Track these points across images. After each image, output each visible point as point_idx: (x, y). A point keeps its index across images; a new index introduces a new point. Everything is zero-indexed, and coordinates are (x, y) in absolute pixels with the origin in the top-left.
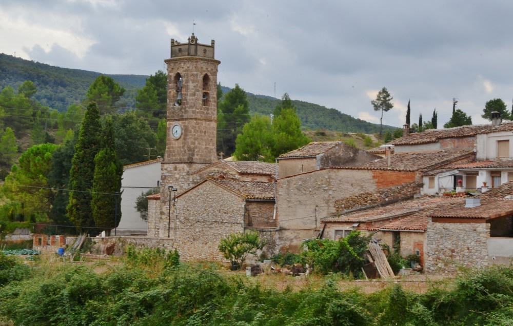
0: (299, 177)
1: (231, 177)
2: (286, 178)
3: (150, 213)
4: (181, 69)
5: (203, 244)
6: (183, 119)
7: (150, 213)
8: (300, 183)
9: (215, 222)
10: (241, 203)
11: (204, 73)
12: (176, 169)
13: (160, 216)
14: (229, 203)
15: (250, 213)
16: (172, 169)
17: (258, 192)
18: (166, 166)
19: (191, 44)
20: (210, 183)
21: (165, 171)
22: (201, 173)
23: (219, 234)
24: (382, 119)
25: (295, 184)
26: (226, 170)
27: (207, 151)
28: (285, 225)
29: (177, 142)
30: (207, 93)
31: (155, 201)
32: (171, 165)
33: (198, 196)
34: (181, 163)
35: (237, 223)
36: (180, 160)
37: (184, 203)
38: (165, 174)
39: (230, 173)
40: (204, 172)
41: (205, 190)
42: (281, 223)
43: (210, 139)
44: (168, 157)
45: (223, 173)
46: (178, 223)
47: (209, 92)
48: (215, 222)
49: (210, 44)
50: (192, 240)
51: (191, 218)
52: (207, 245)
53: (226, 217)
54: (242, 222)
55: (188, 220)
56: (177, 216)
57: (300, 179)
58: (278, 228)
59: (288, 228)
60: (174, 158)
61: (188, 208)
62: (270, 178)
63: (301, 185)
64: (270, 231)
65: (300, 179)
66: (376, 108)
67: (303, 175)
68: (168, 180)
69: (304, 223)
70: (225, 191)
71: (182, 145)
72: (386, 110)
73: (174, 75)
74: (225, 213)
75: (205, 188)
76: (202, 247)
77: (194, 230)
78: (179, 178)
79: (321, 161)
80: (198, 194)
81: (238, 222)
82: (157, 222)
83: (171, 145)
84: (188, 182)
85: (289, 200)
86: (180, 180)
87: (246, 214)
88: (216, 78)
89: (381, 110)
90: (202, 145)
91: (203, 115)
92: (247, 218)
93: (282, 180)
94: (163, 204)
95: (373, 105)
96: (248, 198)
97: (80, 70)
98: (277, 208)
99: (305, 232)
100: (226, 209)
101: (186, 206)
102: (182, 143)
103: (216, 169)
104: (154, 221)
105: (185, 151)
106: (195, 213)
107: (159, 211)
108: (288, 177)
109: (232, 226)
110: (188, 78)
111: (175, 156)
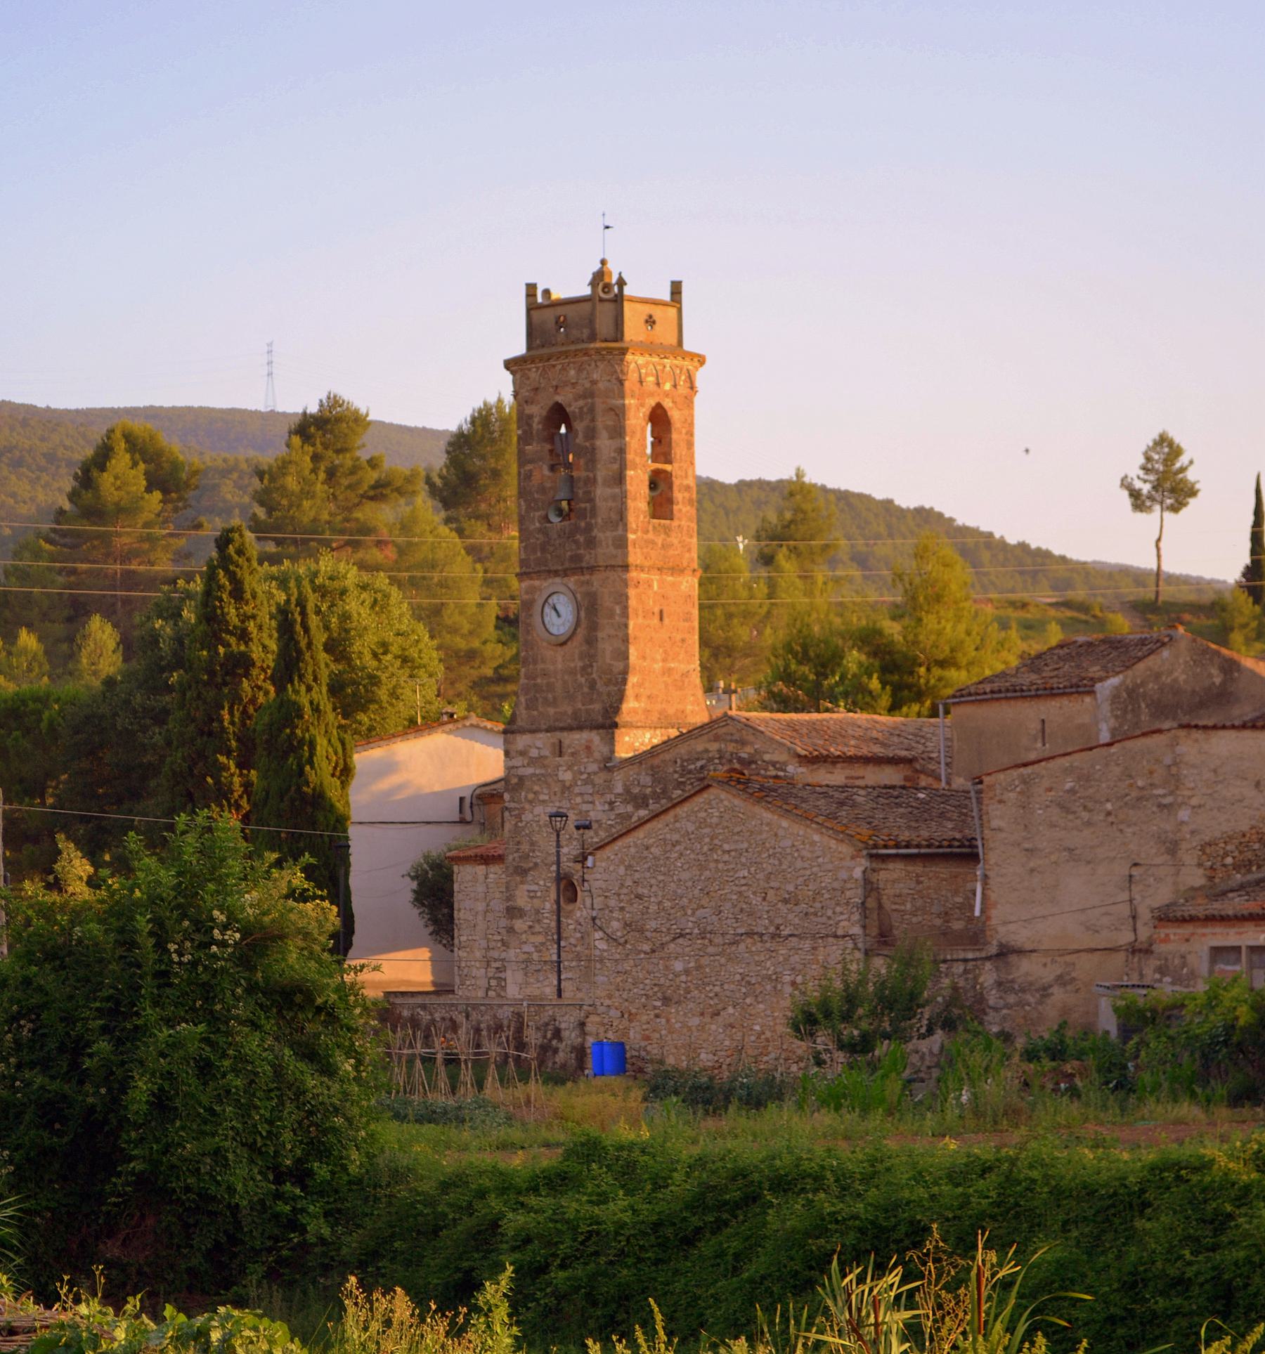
0: (1065, 762)
1: (773, 773)
2: (1017, 766)
3: (462, 915)
4: (568, 389)
5: (702, 1014)
6: (581, 570)
7: (462, 915)
8: (1068, 786)
9: (750, 934)
10: (848, 863)
11: (651, 402)
12: (560, 750)
13: (504, 922)
14: (799, 864)
15: (885, 900)
16: (546, 753)
17: (901, 821)
18: (522, 741)
19: (601, 300)
20: (723, 795)
21: (518, 761)
22: (656, 761)
23: (769, 977)
24: (1162, 545)
25: (1050, 790)
26: (749, 749)
27: (669, 681)
28: (1020, 936)
29: (560, 651)
30: (665, 471)
31: (481, 869)
32: (541, 735)
33: (678, 842)
34: (580, 728)
35: (836, 936)
36: (575, 715)
37: (622, 870)
38: (521, 771)
39: (767, 757)
40: (667, 757)
41: (702, 824)
42: (1002, 929)
43: (678, 637)
44: (527, 708)
45: (740, 760)
46: (602, 945)
47: (668, 467)
48: (750, 934)
49: (666, 296)
50: (658, 1004)
51: (652, 924)
52: (720, 1019)
53: (790, 916)
54: (856, 930)
55: (641, 931)
56: (594, 919)
57: (1068, 771)
58: (993, 950)
59: (1028, 947)
60: (551, 711)
61: (640, 890)
62: (909, 773)
63: (1072, 791)
64: (965, 960)
65: (1068, 771)
66: (1139, 501)
67: (1077, 756)
68: (531, 790)
69: (1088, 928)
70: (785, 823)
71: (580, 664)
72: (1175, 509)
73: (544, 413)
74: (786, 901)
75: (703, 814)
76: (701, 1028)
77: (667, 968)
78: (574, 783)
79: (1113, 703)
80: (676, 837)
81: (840, 932)
82: (492, 944)
83: (540, 666)
84: (609, 797)
85: (1027, 846)
86: (577, 790)
87: (871, 903)
88: (692, 416)
89: (1157, 508)
90: (654, 660)
91: (653, 553)
92: (875, 916)
93: (1001, 776)
94: (518, 879)
95: (1126, 493)
96: (875, 846)
97: (190, 409)
98: (986, 877)
99: (1096, 957)
100: (791, 888)
101: (629, 883)
102: (581, 658)
103: (714, 747)
104: (484, 943)
105: (592, 685)
106: (667, 904)
107: (498, 905)
108: (1025, 765)
109: (814, 948)
110: (593, 420)
111: (554, 703)
